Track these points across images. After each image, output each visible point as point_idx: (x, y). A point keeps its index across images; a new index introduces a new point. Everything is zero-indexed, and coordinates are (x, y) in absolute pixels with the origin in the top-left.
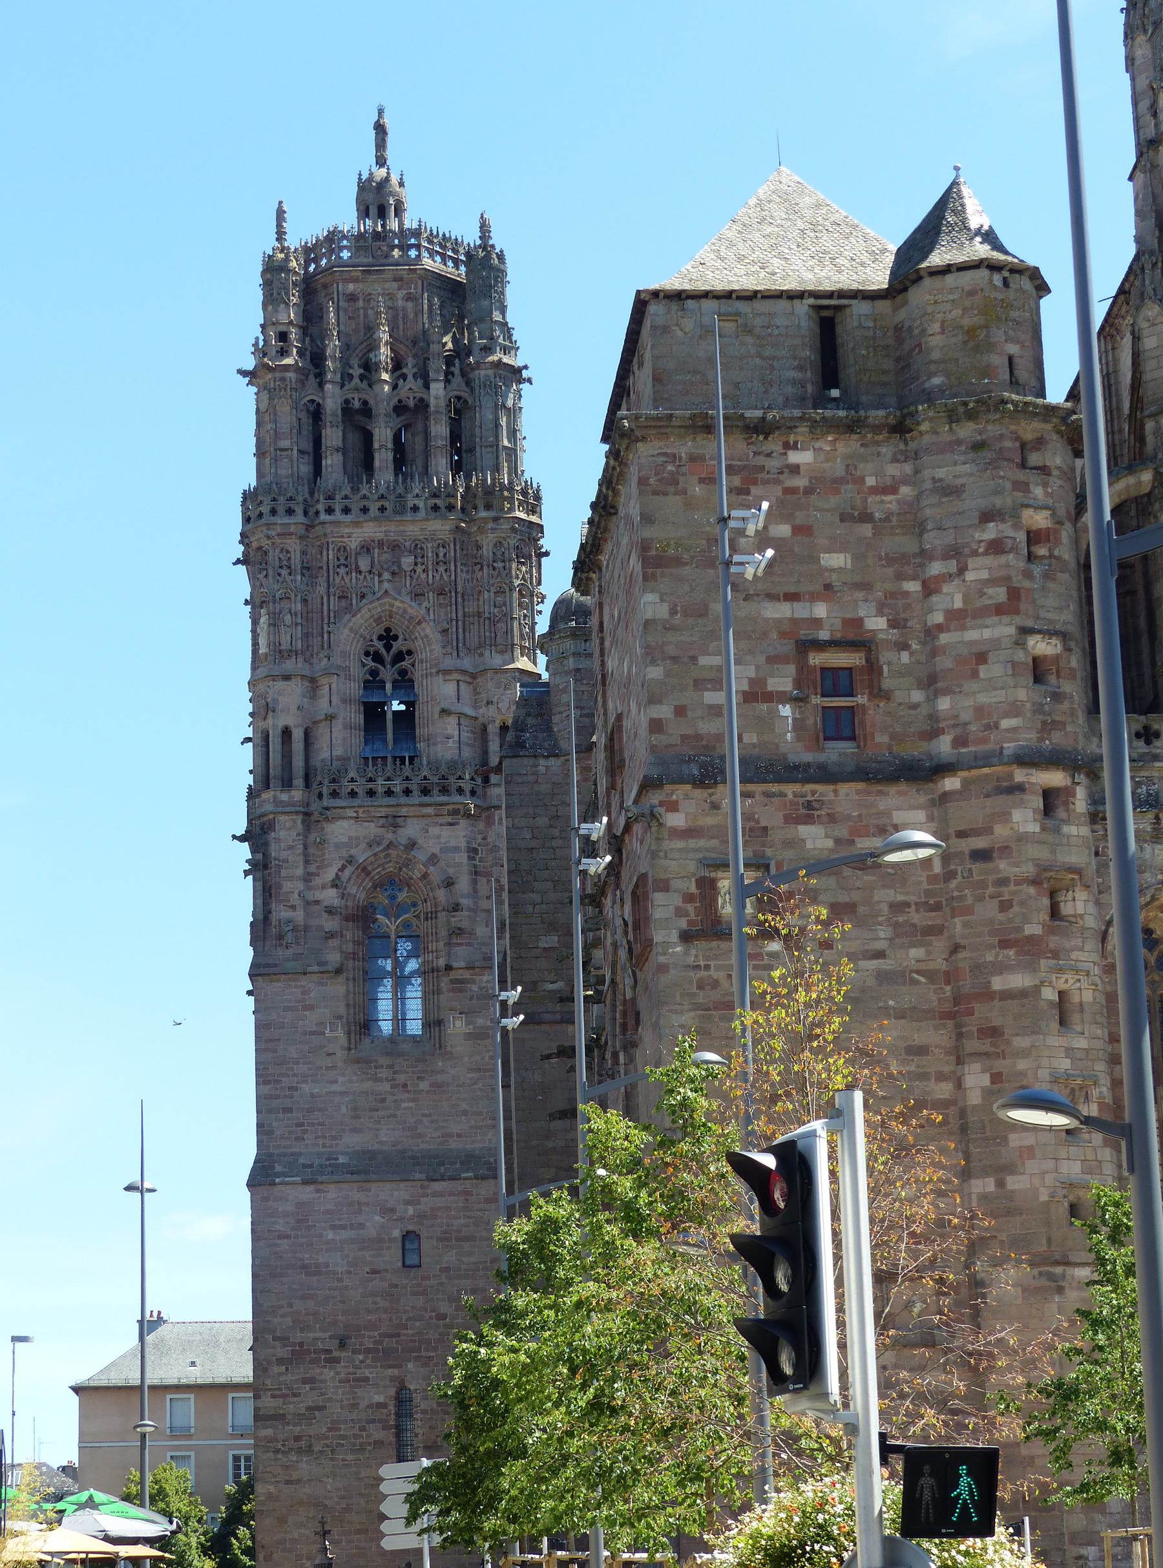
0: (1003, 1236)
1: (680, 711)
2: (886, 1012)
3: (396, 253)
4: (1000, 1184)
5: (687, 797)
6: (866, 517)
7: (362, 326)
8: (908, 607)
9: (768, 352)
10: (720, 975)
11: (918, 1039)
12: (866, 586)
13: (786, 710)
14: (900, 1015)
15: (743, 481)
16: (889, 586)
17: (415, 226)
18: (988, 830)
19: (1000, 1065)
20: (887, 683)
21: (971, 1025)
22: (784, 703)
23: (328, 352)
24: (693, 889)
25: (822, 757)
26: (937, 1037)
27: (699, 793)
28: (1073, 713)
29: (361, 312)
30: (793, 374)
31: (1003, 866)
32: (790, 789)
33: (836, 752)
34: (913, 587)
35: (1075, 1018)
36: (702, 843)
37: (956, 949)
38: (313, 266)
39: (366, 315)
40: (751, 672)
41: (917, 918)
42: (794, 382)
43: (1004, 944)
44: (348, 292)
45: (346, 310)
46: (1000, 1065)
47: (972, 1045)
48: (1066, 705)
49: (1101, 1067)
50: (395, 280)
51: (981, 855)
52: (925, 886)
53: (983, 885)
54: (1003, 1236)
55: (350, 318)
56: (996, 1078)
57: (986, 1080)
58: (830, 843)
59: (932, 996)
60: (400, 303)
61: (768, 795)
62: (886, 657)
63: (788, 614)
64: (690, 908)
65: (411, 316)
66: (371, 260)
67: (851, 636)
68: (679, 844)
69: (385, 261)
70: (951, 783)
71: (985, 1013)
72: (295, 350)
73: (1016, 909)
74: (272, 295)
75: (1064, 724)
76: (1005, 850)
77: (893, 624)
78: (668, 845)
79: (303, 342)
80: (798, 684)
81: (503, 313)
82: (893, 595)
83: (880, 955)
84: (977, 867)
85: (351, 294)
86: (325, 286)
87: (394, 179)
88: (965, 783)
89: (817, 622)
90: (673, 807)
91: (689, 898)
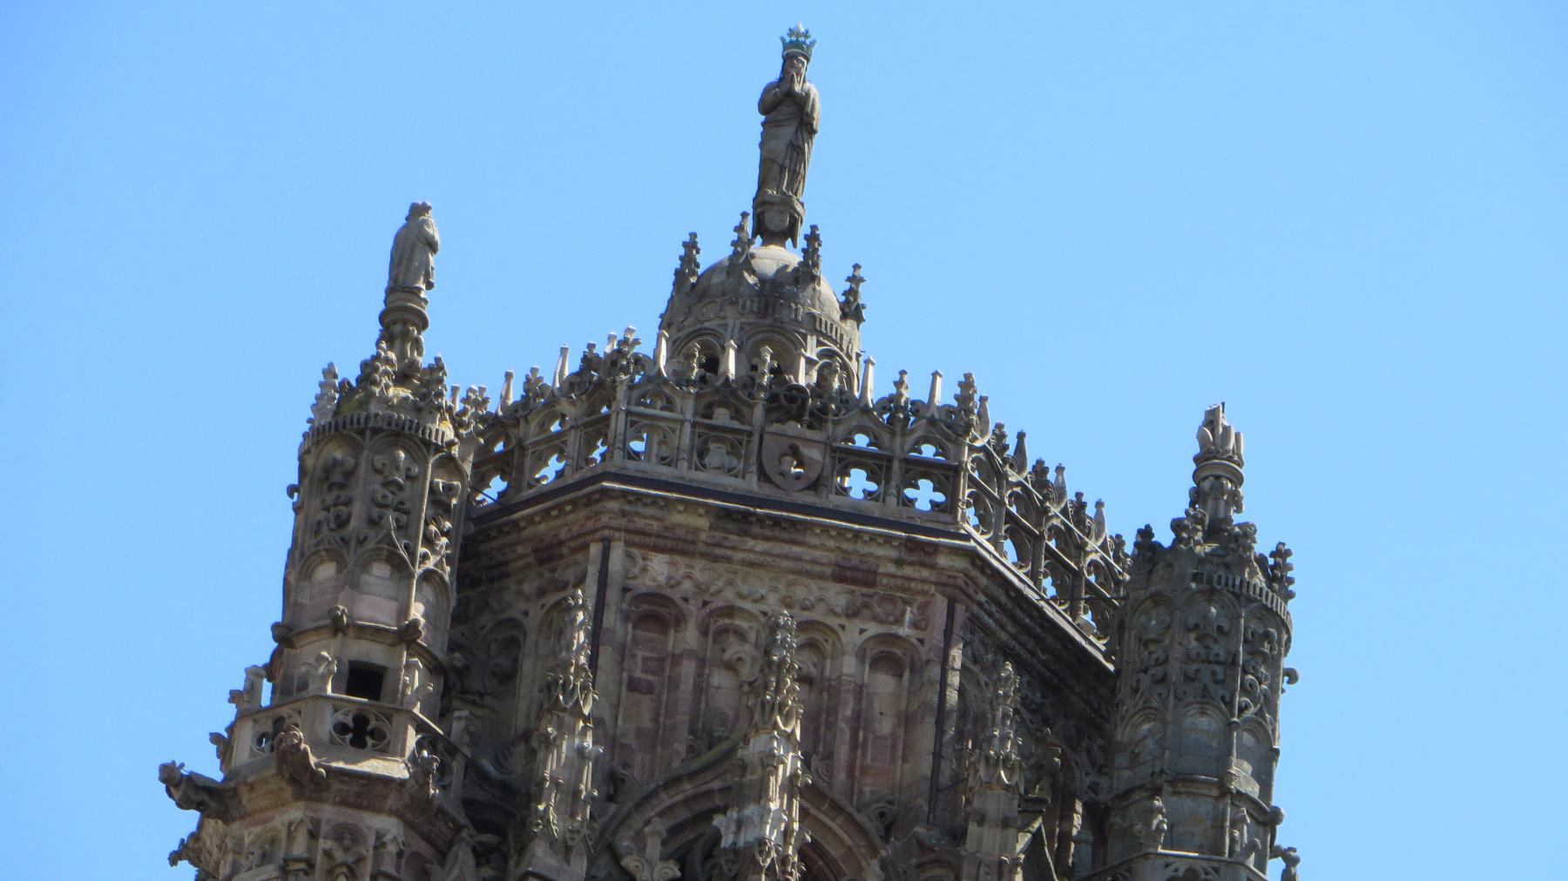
3: (857, 482)
7: (683, 718)
17: (945, 396)
23: (551, 767)
29: (688, 668)
38: (497, 485)
39: (701, 688)
44: (645, 584)
45: (623, 653)
50: (842, 575)
55: (633, 686)
60: (849, 665)
65: (885, 726)
66: (751, 484)
69: (809, 498)
72: (412, 738)
74: (342, 522)
79: (443, 715)
81: (1264, 779)
85: (655, 597)
86: (547, 554)
87: (829, 290)
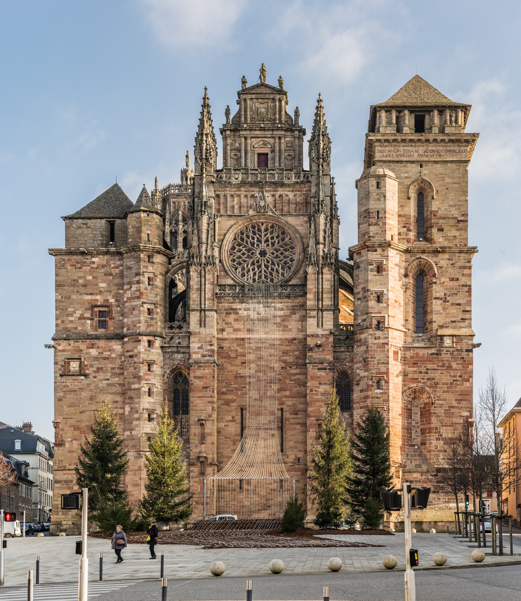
0: (131, 445)
2: (109, 393)
4: (131, 433)
6: (111, 274)
9: (94, 232)
10: (69, 384)
11: (116, 399)
12: (110, 292)
13: (89, 322)
14: (112, 394)
16: (116, 291)
18: (133, 351)
19: (132, 406)
20: (113, 315)
21: (127, 396)
25: (96, 333)
26: (119, 398)
27: (66, 341)
28: (156, 323)
30: (100, 238)
31: (135, 359)
32: (88, 341)
33: (101, 331)
35: (152, 395)
36: (66, 353)
40: (81, 312)
41: (117, 371)
42: (101, 240)
43: (135, 377)
46: (132, 406)
47: (127, 401)
48: (154, 321)
51: (131, 357)
53: (131, 363)
54: (131, 445)
56: (131, 408)
57: (129, 409)
58: (97, 353)
59: (119, 389)
61: (83, 342)
62: (114, 308)
64: (63, 368)
67: (106, 304)
68: (61, 353)
70: (126, 339)
71: (130, 393)
73: (137, 369)
75: (153, 325)
76: (136, 355)
77: (116, 301)
80: (92, 315)
82: (116, 294)
83: (108, 380)
84: (130, 359)
88: (129, 339)
89: (97, 300)
91: (62, 366)
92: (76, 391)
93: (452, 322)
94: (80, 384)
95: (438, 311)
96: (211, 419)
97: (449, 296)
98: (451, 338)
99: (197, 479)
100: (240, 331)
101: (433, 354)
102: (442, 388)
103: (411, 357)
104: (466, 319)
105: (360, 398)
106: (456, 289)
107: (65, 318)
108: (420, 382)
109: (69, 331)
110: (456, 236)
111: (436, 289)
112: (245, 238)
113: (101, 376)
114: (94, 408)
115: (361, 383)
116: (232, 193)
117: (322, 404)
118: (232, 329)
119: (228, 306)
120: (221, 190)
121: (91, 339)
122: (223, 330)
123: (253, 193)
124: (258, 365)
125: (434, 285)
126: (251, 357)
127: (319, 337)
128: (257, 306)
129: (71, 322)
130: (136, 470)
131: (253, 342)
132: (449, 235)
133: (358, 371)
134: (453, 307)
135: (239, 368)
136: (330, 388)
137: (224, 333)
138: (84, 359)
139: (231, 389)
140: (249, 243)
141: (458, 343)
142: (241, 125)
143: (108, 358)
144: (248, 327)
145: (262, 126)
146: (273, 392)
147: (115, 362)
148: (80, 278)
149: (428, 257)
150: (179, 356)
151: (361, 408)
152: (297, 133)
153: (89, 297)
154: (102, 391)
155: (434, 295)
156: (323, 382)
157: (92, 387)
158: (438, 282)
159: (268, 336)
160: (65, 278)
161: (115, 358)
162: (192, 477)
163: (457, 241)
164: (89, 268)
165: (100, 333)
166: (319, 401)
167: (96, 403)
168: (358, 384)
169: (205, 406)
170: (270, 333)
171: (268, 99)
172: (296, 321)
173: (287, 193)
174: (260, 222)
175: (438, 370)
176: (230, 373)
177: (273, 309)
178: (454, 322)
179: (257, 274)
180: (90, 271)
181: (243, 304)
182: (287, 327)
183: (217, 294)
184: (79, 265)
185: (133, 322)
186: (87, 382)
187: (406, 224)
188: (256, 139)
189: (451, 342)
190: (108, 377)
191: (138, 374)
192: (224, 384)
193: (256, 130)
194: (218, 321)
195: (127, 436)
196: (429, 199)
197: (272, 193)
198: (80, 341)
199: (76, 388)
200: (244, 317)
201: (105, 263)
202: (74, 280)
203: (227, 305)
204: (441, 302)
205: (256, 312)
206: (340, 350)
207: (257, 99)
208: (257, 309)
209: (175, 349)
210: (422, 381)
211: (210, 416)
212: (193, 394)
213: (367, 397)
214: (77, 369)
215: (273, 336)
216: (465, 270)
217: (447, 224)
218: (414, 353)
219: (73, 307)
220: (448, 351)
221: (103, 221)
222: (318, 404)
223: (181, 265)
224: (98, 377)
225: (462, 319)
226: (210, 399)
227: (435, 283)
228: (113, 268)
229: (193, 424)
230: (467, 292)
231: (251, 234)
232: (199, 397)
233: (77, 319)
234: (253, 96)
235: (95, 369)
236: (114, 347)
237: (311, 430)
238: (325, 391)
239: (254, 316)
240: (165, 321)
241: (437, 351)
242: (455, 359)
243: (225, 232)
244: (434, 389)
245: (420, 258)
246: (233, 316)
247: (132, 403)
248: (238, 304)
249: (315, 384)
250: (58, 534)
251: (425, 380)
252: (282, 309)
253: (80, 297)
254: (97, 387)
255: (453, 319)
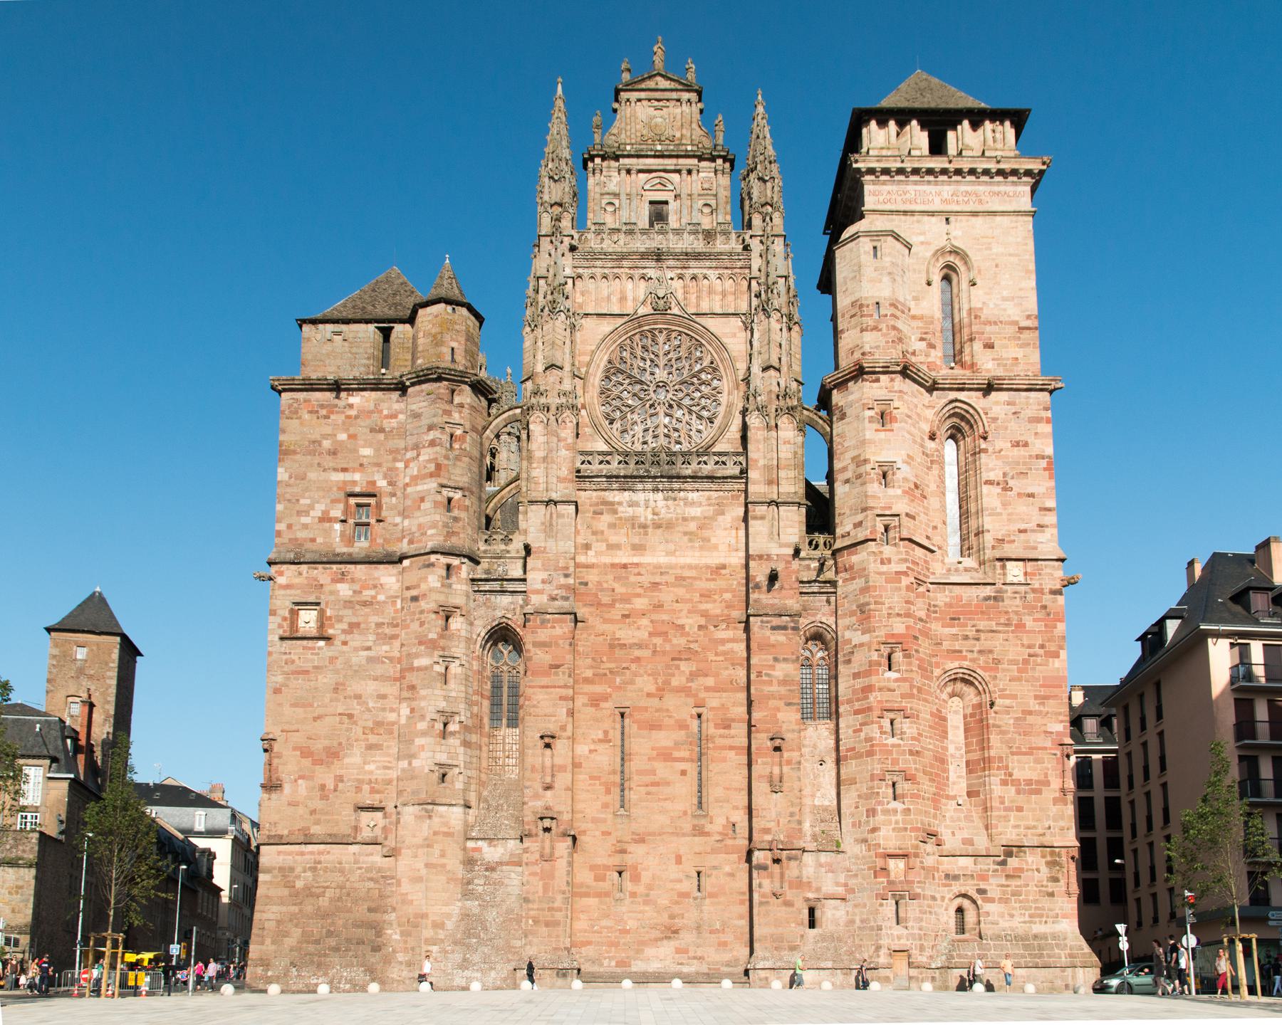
1: (290, 526)
5: (288, 569)
8: (397, 475)
9: (354, 350)
10: (292, 656)
13: (338, 526)
15: (328, 412)
21: (405, 683)
22: (335, 522)
24: (287, 615)
32: (334, 567)
34: (401, 465)
36: (293, 592)
37: (402, 645)
42: (365, 366)
46: (414, 704)
49: (462, 706)
52: (392, 615)
58: (351, 593)
63: (342, 479)
68: (282, 592)
78: (277, 592)
90: (281, 574)
91: (285, 619)
92: (307, 672)
93: (1020, 531)
94: (316, 657)
95: (992, 509)
96: (565, 734)
97: (1013, 478)
98: (1021, 563)
99: (537, 869)
100: (620, 549)
101: (987, 598)
102: (1008, 670)
103: (946, 604)
104: (1047, 526)
105: (854, 692)
106: (1025, 464)
107: (293, 520)
108: (965, 658)
109: (301, 545)
110: (1017, 359)
111: (987, 465)
112: (629, 361)
113: (356, 640)
114: (340, 710)
115: (856, 658)
116: (606, 271)
117: (781, 704)
118: (604, 544)
119: (597, 497)
120: (585, 264)
121: (340, 563)
122: (587, 547)
123: (645, 271)
124: (652, 621)
125: (983, 455)
126: (640, 603)
127: (772, 559)
128: (651, 495)
129: (305, 526)
130: (419, 846)
131: (643, 571)
132: (1005, 356)
133: (848, 634)
134: (1021, 500)
135: (618, 626)
136: (795, 670)
137: (590, 553)
138: (327, 603)
139: (602, 671)
140: (636, 371)
141: (1034, 574)
142: (622, 147)
143: (371, 603)
144: (636, 540)
145: (659, 148)
146: (684, 679)
147: (383, 612)
148: (325, 436)
149: (969, 398)
150: (505, 600)
151: (857, 712)
152: (720, 161)
153: (340, 476)
154: (357, 672)
155: (985, 476)
156: (781, 657)
157: (339, 664)
158: (990, 449)
159: (673, 560)
160: (298, 438)
161: (384, 602)
162: (527, 864)
163: (1021, 367)
164: (343, 417)
165: (357, 550)
166: (774, 698)
167: (345, 698)
168: (849, 662)
169: (554, 705)
170: (677, 553)
171: (668, 100)
172: (726, 529)
173: (705, 271)
174: (655, 329)
175: (999, 632)
176: (601, 638)
177: (682, 503)
178: (1024, 531)
179: (651, 430)
180: (344, 423)
181: (626, 494)
182: (709, 541)
183: (578, 471)
184: (324, 412)
185: (420, 526)
186: (330, 654)
187: (926, 333)
188: (647, 175)
189: (1022, 574)
190: (370, 644)
191: (426, 636)
192: (589, 661)
193: (647, 156)
194: (579, 527)
195: (403, 770)
196: (964, 285)
197: (679, 271)
198: (320, 566)
199: (308, 666)
200: (627, 519)
201: (372, 407)
202: (314, 442)
203: (595, 494)
204: (998, 490)
205: (650, 509)
206: (809, 591)
207: (649, 100)
208: (652, 504)
209: (496, 586)
210: (970, 655)
211: (563, 728)
212: (532, 681)
213: (868, 689)
214: (313, 624)
215: (682, 561)
216: (1039, 425)
217: (999, 333)
218: (952, 597)
219: (310, 498)
220: (1016, 593)
221: (371, 327)
222: (773, 703)
223: (511, 413)
224: (351, 643)
225: (1039, 526)
226: (564, 692)
227: (985, 451)
228: (387, 417)
229: (531, 745)
230: (1045, 469)
231: (639, 352)
232: (543, 687)
233: (317, 520)
234: (643, 95)
235: (345, 626)
236: (384, 580)
237: (759, 761)
238: (786, 675)
239: (646, 518)
240: (480, 528)
241: (997, 592)
242: (1030, 609)
243: (593, 348)
244: (993, 674)
245: (956, 400)
246: (606, 518)
247: (414, 699)
248: (616, 492)
249: (765, 660)
250: (261, 987)
251: (975, 655)
252: (700, 504)
253: (324, 476)
254: (348, 663)
255: (1023, 527)
